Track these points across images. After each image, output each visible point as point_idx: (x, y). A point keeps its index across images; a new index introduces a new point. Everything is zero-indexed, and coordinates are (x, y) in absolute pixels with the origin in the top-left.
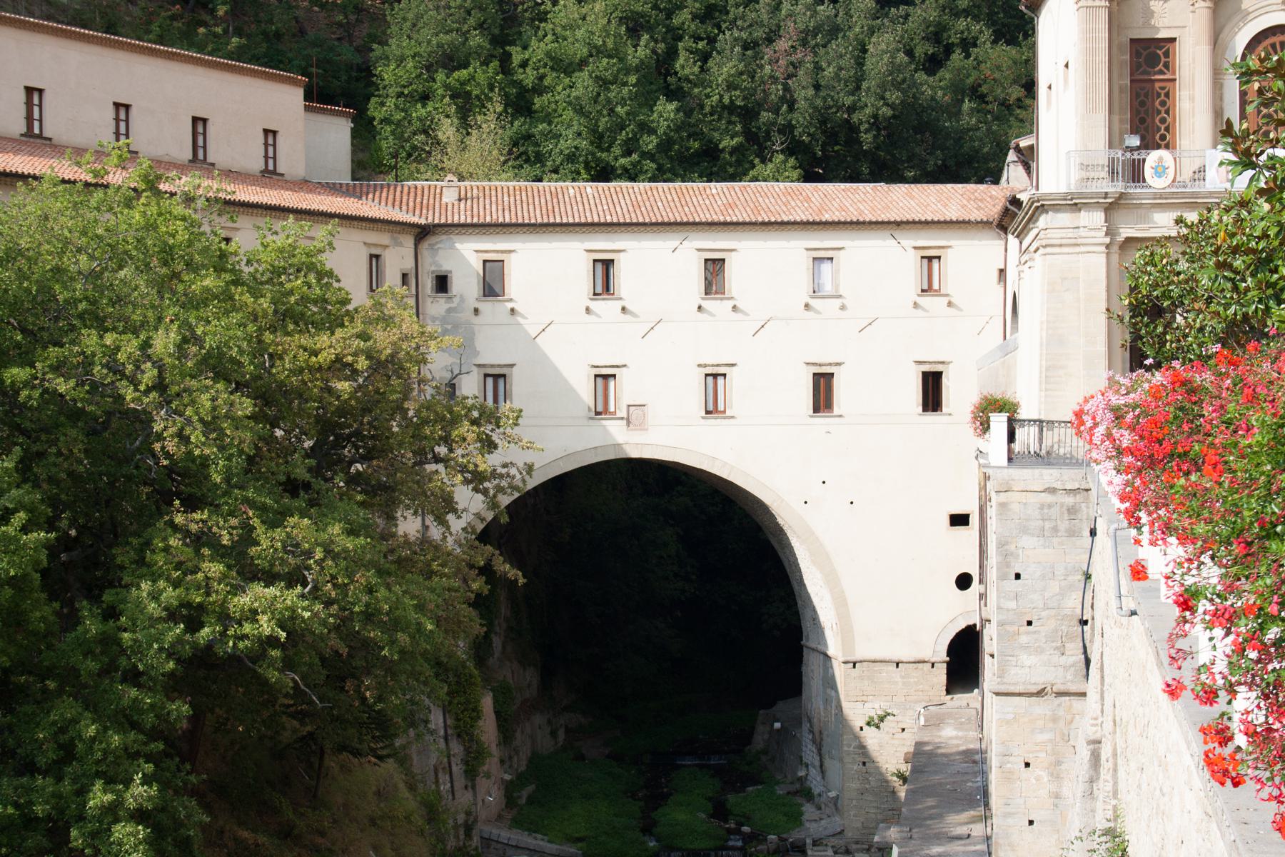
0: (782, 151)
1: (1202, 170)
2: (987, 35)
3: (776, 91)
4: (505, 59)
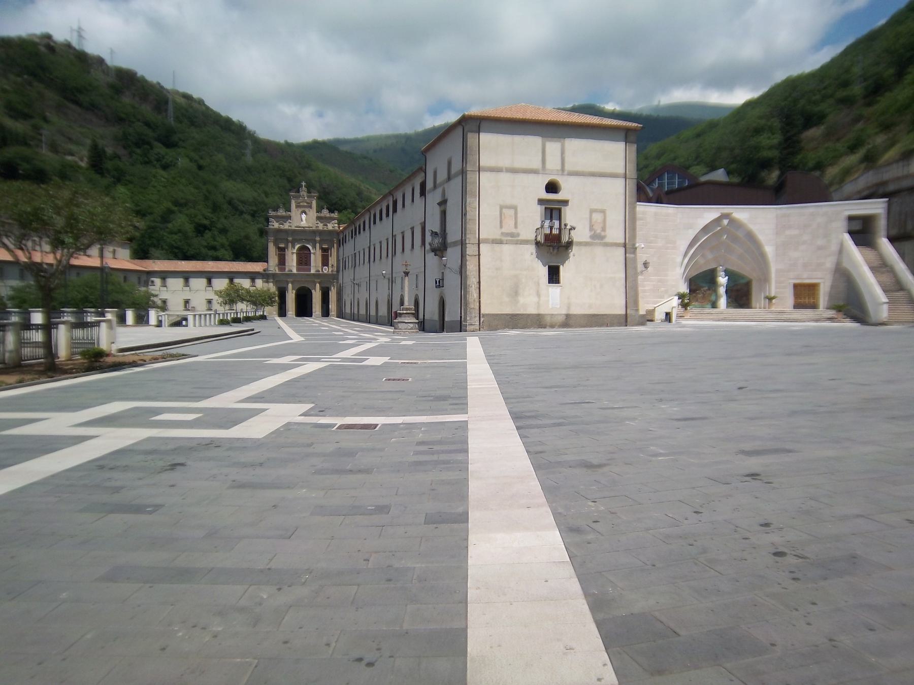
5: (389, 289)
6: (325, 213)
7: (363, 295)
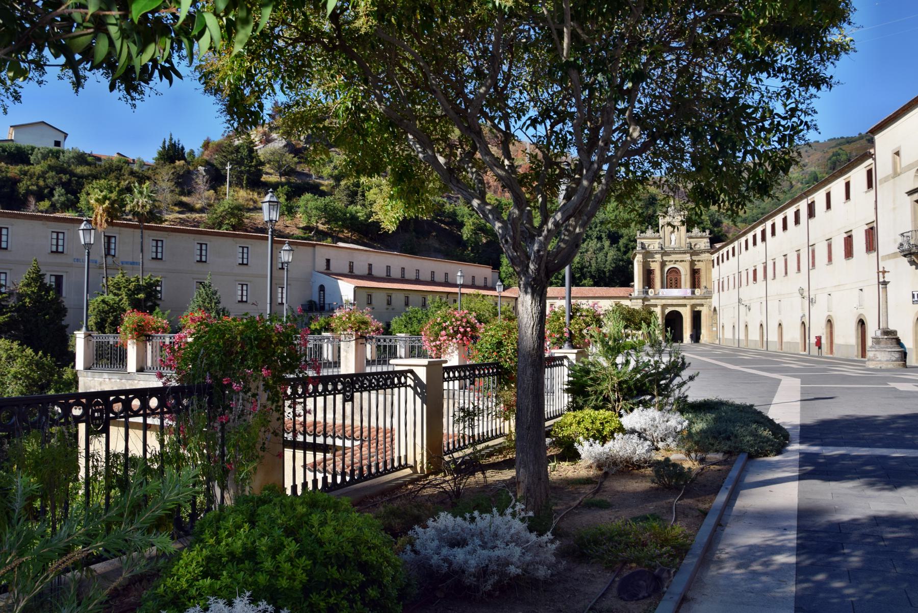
3: (587, 264)
5: (803, 309)
7: (755, 318)
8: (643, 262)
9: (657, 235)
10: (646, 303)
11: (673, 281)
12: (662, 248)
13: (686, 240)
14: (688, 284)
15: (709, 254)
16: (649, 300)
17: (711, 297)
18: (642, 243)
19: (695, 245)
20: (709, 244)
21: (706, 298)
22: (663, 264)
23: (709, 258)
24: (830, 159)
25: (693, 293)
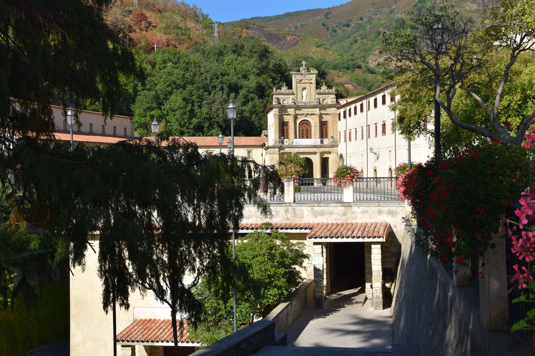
0: (217, 127)
1: (293, 142)
2: (257, 97)
4: (160, 109)
6: (324, 88)
8: (279, 115)
9: (290, 91)
10: (281, 151)
11: (305, 131)
12: (295, 103)
13: (315, 96)
14: (318, 134)
15: (336, 109)
16: (283, 149)
17: (337, 146)
18: (278, 99)
19: (323, 100)
20: (335, 100)
21: (333, 146)
22: (296, 117)
23: (336, 112)
24: (416, 6)
25: (322, 142)
